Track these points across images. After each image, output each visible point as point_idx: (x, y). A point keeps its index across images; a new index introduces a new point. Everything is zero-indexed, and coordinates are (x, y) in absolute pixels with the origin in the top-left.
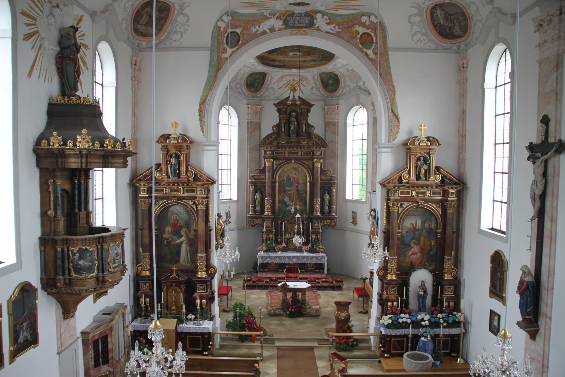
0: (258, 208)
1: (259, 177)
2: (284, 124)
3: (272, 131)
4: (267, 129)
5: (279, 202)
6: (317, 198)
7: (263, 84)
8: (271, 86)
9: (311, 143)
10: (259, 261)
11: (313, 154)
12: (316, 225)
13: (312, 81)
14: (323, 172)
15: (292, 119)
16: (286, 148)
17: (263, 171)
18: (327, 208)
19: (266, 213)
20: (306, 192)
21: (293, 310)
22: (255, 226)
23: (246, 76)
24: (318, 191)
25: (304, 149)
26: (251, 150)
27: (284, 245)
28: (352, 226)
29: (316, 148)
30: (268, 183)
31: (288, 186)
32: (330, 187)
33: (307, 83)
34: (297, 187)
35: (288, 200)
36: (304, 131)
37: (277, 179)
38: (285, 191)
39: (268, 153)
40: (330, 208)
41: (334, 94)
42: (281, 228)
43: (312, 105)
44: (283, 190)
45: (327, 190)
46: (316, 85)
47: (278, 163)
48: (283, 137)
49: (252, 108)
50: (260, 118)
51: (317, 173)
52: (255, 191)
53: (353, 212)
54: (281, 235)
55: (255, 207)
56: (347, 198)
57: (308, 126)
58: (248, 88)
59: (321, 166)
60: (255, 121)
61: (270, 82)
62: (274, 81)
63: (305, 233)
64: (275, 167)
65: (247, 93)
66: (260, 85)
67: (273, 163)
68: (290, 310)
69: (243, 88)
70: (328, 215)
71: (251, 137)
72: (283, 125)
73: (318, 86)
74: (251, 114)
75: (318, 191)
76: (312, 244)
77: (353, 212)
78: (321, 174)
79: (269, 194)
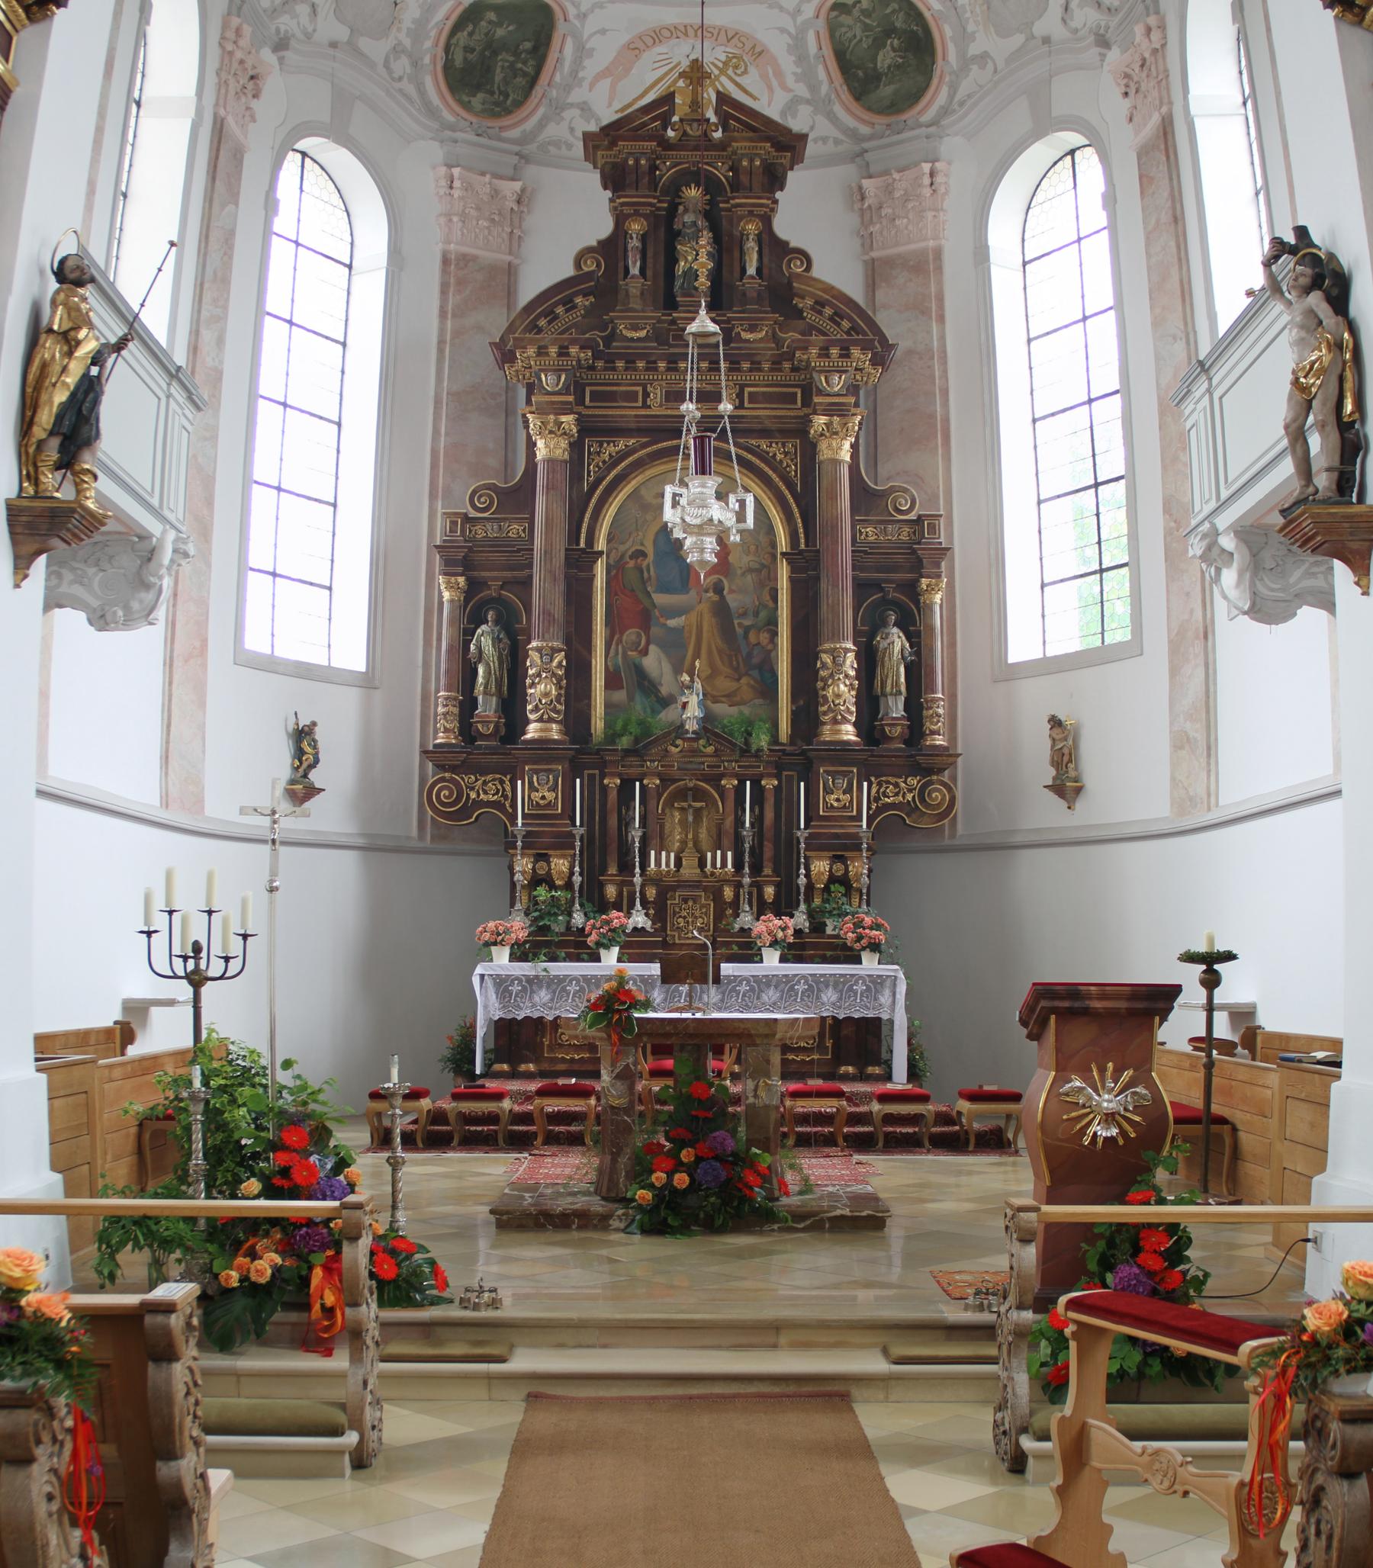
0: (487, 708)
1: (492, 531)
2: (644, 239)
3: (569, 271)
4: (548, 264)
5: (613, 681)
6: (837, 636)
8: (576, 96)
9: (791, 336)
10: (488, 1008)
11: (809, 390)
12: (831, 799)
13: (788, 64)
14: (865, 498)
15: (688, 218)
16: (651, 367)
17: (516, 498)
18: (896, 708)
19: (533, 731)
20: (772, 623)
21: (681, 1180)
22: (464, 812)
24: (842, 603)
25: (756, 367)
26: (460, 403)
27: (639, 919)
28: (1046, 813)
29: (824, 353)
30: (547, 553)
31: (665, 589)
32: (912, 590)
33: (764, 77)
34: (718, 589)
35: (667, 668)
36: (751, 270)
37: (601, 544)
38: (645, 619)
39: (548, 381)
40: (915, 707)
41: (909, 115)
42: (625, 823)
43: (788, 146)
44: (633, 613)
45: (897, 605)
46: (813, 88)
47: (610, 450)
48: (635, 304)
49: (468, 187)
50: (515, 240)
51: (833, 496)
52: (471, 614)
53: (1055, 722)
54: (626, 868)
55: (467, 706)
56: (1012, 659)
57: (776, 249)
58: (452, 89)
59: (855, 455)
60: (487, 255)
61: (574, 73)
62: (592, 67)
63: (768, 851)
64: (590, 472)
65: (448, 111)
66: (520, 81)
67: (576, 447)
68: (659, 1178)
70: (906, 747)
71: (457, 333)
72: (634, 243)
73: (824, 88)
74: (464, 217)
75: (842, 603)
76: (811, 914)
77: (1055, 722)
78: (855, 509)
79: (547, 614)
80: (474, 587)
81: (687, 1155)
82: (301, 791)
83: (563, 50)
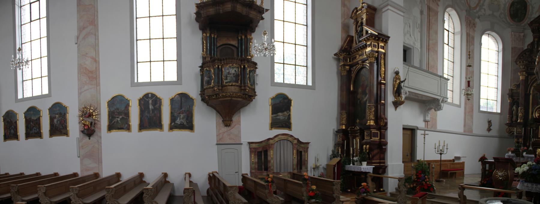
7: (525, 14)
23: (508, 5)
37: (531, 92)
67: (527, 78)
69: (507, 18)
80: (513, 99)
81: (487, 179)
82: (489, 130)
83: (530, 8)
